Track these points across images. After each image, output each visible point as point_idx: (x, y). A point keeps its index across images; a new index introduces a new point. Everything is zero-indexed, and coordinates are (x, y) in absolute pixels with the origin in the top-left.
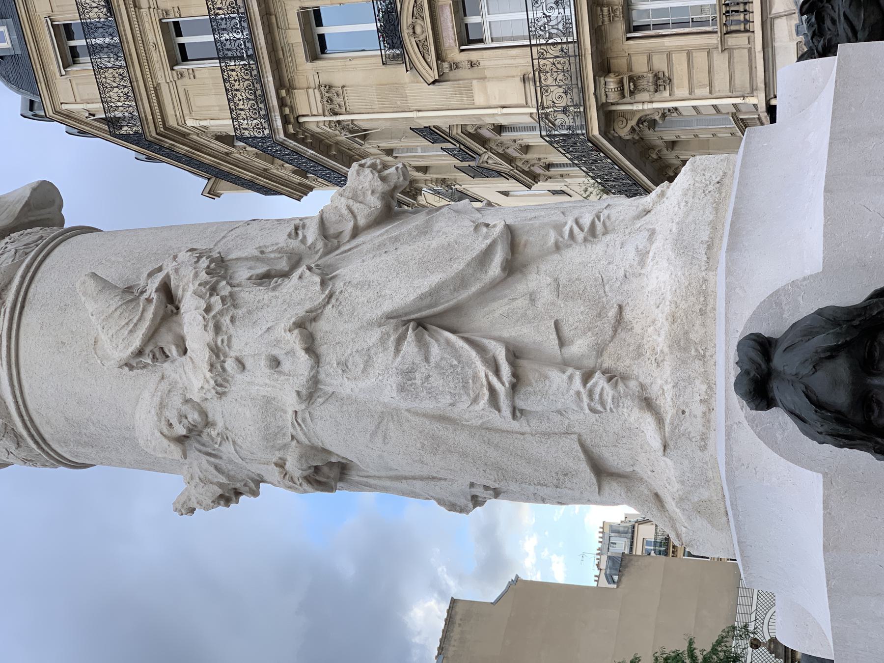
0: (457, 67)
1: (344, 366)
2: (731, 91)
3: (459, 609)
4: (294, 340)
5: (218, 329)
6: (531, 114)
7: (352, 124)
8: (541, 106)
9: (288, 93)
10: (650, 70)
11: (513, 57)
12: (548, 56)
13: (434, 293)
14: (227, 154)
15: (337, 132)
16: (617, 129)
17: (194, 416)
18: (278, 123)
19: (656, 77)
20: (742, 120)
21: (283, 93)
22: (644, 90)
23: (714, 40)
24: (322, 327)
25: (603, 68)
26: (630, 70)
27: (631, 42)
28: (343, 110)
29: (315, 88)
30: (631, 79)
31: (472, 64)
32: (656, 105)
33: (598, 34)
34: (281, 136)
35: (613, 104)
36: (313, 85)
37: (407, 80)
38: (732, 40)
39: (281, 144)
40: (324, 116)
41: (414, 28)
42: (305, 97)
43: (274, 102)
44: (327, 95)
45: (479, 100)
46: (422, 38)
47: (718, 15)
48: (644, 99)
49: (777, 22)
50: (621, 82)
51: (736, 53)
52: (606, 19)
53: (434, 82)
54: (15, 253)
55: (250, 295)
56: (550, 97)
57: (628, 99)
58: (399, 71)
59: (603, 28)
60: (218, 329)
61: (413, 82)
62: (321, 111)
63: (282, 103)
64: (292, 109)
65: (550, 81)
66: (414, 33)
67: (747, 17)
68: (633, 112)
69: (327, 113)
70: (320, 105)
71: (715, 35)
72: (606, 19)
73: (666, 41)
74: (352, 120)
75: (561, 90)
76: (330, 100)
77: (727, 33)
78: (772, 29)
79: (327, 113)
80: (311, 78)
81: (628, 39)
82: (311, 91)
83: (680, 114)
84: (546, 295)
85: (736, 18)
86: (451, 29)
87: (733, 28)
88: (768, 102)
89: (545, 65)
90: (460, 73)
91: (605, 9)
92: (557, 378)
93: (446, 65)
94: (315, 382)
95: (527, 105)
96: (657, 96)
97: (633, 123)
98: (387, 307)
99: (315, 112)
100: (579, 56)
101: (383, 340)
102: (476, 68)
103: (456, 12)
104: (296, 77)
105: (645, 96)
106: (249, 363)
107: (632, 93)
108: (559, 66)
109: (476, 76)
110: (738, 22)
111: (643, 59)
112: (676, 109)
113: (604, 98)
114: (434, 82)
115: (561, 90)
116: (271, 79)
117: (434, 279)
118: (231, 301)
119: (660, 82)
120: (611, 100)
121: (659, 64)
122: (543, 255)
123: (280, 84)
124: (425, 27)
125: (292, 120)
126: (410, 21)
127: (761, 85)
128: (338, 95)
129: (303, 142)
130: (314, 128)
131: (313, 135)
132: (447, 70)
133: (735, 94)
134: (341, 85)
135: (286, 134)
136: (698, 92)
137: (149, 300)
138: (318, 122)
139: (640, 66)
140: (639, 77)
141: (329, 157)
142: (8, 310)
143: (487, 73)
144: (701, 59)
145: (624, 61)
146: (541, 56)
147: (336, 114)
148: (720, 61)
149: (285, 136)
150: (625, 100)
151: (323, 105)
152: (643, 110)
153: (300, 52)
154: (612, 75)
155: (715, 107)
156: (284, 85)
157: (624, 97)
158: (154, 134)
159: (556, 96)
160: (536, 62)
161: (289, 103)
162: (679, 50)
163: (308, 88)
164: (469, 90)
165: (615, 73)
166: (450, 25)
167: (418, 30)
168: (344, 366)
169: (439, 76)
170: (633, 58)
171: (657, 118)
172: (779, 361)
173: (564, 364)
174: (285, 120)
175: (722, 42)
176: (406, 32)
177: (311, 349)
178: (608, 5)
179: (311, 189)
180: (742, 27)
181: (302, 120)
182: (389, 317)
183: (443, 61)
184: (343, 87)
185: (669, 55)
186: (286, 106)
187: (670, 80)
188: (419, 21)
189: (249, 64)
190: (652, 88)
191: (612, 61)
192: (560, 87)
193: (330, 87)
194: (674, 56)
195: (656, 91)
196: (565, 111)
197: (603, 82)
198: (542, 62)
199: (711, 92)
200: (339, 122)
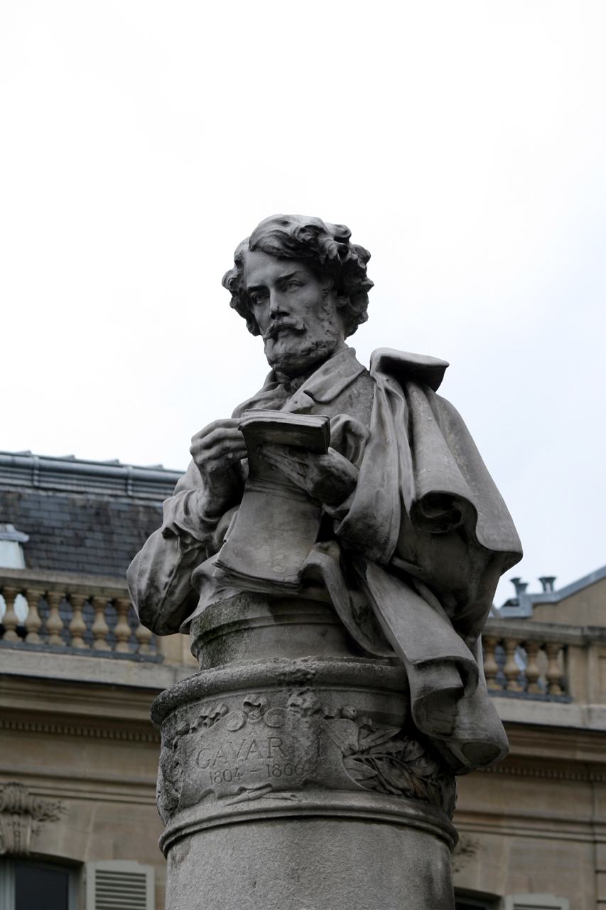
54: (371, 778)
142: (289, 803)
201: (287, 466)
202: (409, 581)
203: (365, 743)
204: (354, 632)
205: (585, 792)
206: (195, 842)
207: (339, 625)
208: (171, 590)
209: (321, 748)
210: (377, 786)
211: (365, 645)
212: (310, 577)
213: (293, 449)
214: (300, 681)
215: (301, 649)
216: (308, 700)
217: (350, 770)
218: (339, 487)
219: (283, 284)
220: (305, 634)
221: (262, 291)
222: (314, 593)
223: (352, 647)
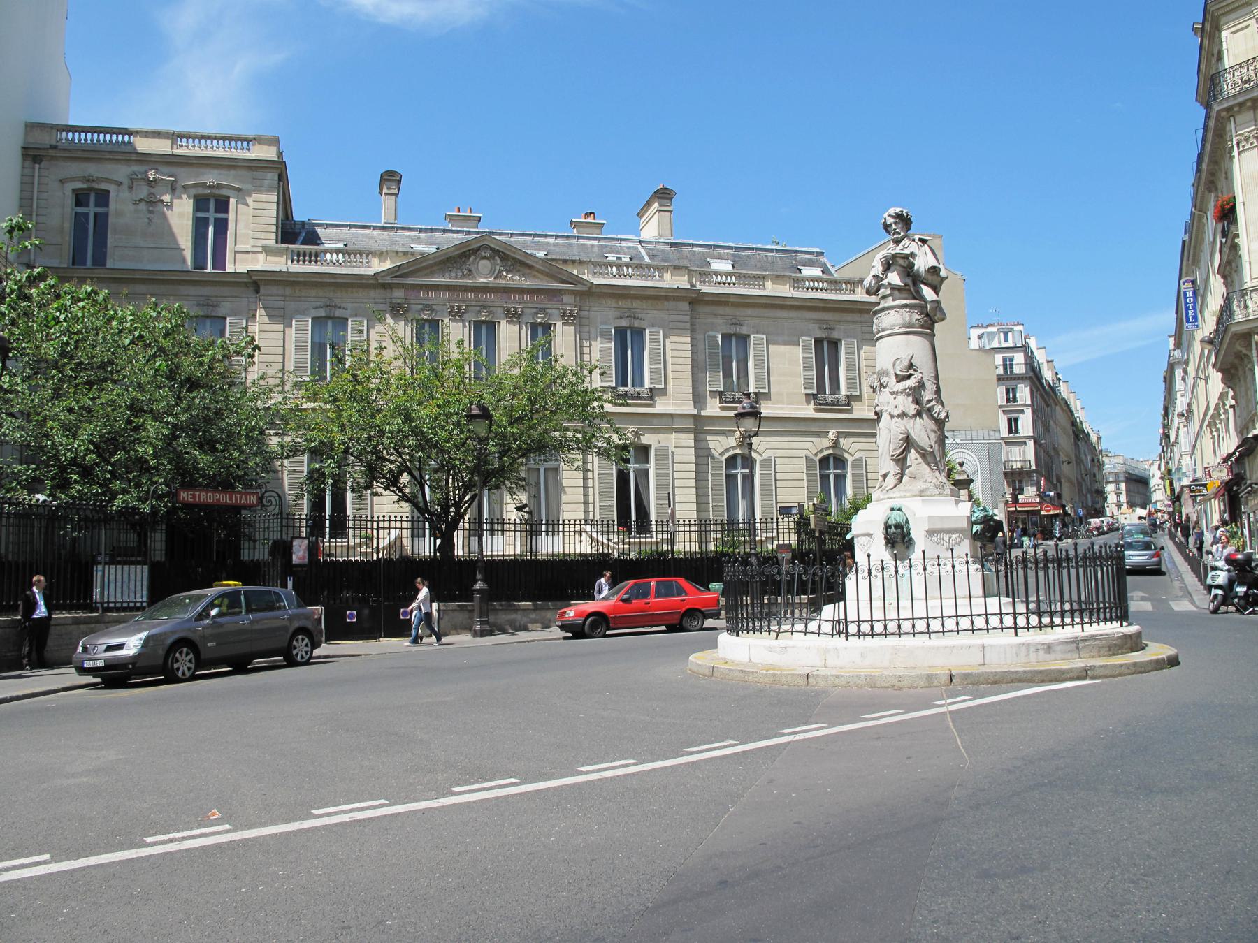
1: (897, 422)
4: (900, 412)
5: (902, 393)
14: (1213, 55)
17: (885, 384)
28: (1241, 149)
55: (910, 398)
60: (902, 393)
64: (1239, 112)
68: (1251, 350)
84: (917, 462)
97: (1244, 351)
135: (1218, 112)
147: (1238, 144)
151: (1242, 134)
158: (1212, 9)
181: (1232, 119)
186: (1240, 107)
201: (901, 262)
202: (925, 284)
203: (919, 317)
207: (912, 293)
210: (922, 327)
213: (903, 258)
219: (895, 223)
221: (891, 225)
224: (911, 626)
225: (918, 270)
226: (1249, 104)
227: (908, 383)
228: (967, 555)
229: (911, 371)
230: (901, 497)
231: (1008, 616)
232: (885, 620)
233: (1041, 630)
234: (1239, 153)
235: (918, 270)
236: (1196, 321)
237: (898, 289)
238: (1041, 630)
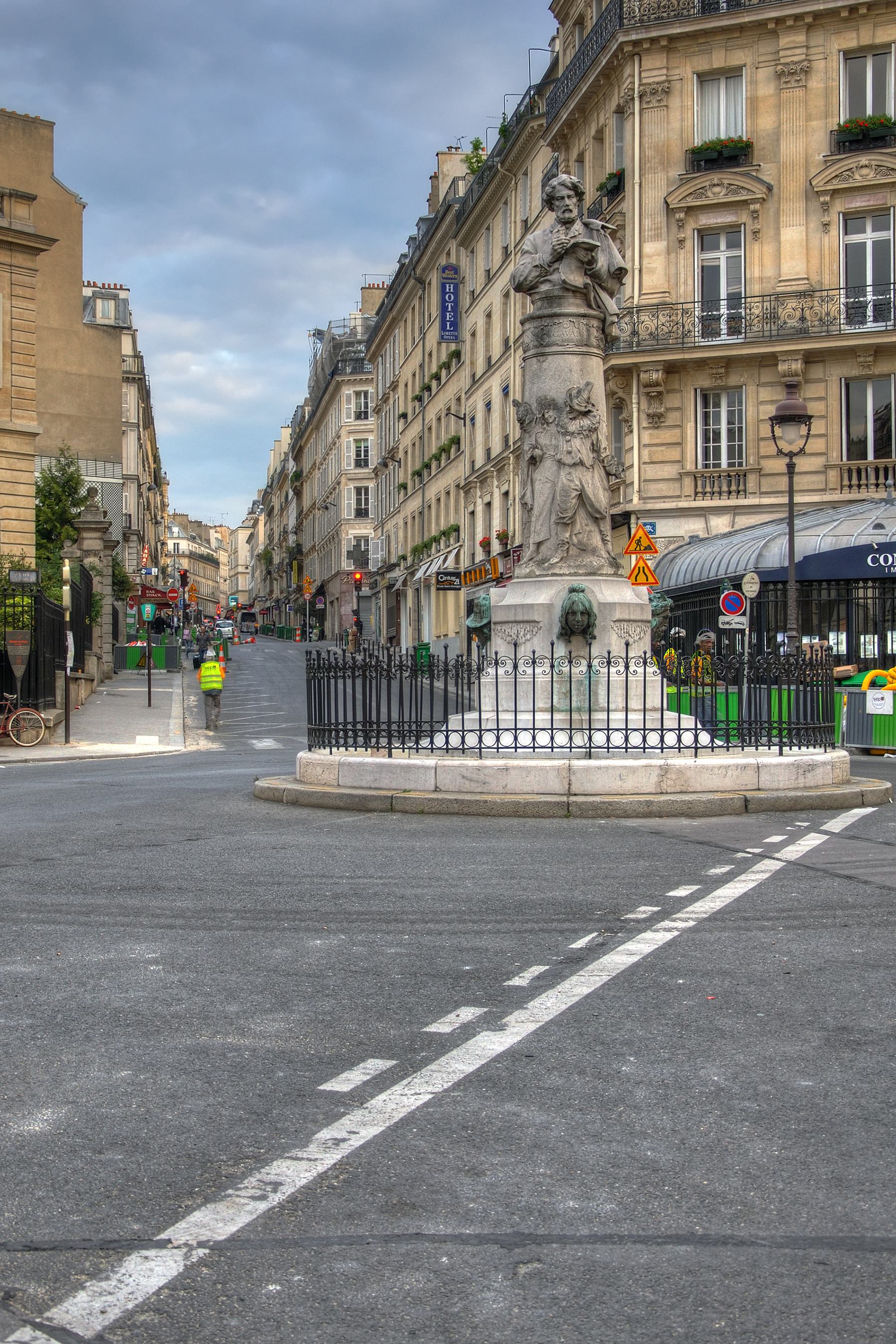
0: (680, 227)
2: (645, 481)
3: (44, 131)
6: (633, 297)
7: (631, 113)
8: (640, 309)
9: (664, 47)
10: (667, 409)
11: (685, 283)
12: (685, 319)
13: (589, 498)
15: (622, 94)
16: (617, 378)
18: (634, 37)
19: (660, 416)
20: (619, 488)
21: (664, 43)
22: (650, 404)
23: (689, 466)
24: (580, 468)
25: (671, 369)
26: (668, 392)
27: (693, 393)
29: (667, 76)
30: (660, 393)
31: (681, 242)
32: (635, 415)
33: (701, 363)
34: (622, 39)
35: (639, 376)
36: (671, 73)
37: (670, 174)
38: (688, 482)
39: (613, 36)
40: (640, 85)
41: (718, 185)
42: (658, 65)
43: (654, 34)
44: (660, 89)
45: (650, 248)
46: (709, 194)
47: (712, 469)
48: (641, 404)
49: (703, 519)
50: (657, 384)
51: (677, 485)
52: (714, 371)
53: (666, 202)
56: (647, 318)
57: (642, 390)
58: (677, 170)
59: (707, 367)
61: (668, 179)
62: (644, 81)
63: (653, 40)
64: (647, 50)
65: (662, 319)
66: (714, 185)
67: (708, 495)
69: (642, 88)
70: (651, 80)
71: (694, 467)
72: (714, 371)
73: (692, 424)
74: (633, 113)
75: (653, 330)
76: (654, 93)
77: (695, 477)
78: (696, 516)
79: (642, 88)
80: (677, 71)
81: (696, 390)
82: (664, 71)
83: (626, 434)
84: (588, 529)
85: (708, 484)
86: (715, 221)
87: (699, 483)
88: (634, 512)
89: (677, 315)
90: (674, 228)
91: (723, 370)
92: (567, 535)
93: (682, 215)
94: (564, 464)
95: (640, 295)
96: (643, 416)
98: (586, 486)
99: (643, 74)
100: (683, 350)
101: (577, 485)
102: (677, 244)
103: (731, 226)
104: (678, 55)
105: (644, 405)
106: (569, 444)
107: (648, 394)
108: (675, 329)
109: (671, 244)
110: (704, 487)
111: (677, 404)
112: (631, 432)
113: (645, 369)
114: (666, 202)
115: (653, 330)
116: (679, 31)
117: (593, 500)
118: (587, 436)
119: (656, 419)
120: (642, 375)
121: (672, 418)
122: (599, 527)
123: (671, 38)
124: (719, 195)
125: (637, 50)
126: (726, 182)
127: (649, 506)
128: (659, 101)
129: (615, 55)
130: (627, 71)
131: (621, 66)
132: (677, 216)
133: (642, 484)
134: (671, 105)
136: (645, 452)
137: (586, 407)
138: (634, 76)
139: (672, 401)
140: (661, 400)
141: (597, 76)
143: (673, 255)
144: (675, 454)
145: (677, 387)
146: (685, 312)
147: (641, 97)
148: (670, 471)
149: (622, 43)
150: (641, 387)
151: (649, 84)
152: (631, 403)
153: (703, 64)
154: (665, 376)
155: (632, 466)
156: (671, 44)
157: (646, 386)
159: (648, 322)
160: (680, 306)
161: (654, 47)
162: (683, 436)
163: (668, 69)
164: (657, 237)
165: (667, 378)
166: (719, 221)
167: (717, 189)
168: (570, 473)
169: (673, 209)
170: (678, 395)
171: (624, 415)
172: (581, 594)
173: (570, 536)
174: (636, 43)
175: (688, 474)
176: (715, 177)
177: (574, 465)
178: (727, 373)
179: (562, 23)
180: (699, 489)
182: (583, 486)
183: (686, 213)
184: (667, 106)
185: (679, 426)
186: (651, 44)
187: (657, 428)
188: (724, 191)
189: (694, 7)
190: (651, 411)
191: (677, 375)
192: (657, 329)
193: (667, 93)
194: (677, 431)
195: (648, 415)
196: (635, 333)
197: (658, 368)
198: (680, 312)
199: (645, 463)
200: (633, 99)
201: (581, 254)
204: (593, 303)
205: (9, 253)
206: (550, 357)
208: (532, 281)
209: (589, 336)
211: (594, 307)
212: (586, 286)
213: (586, 249)
214: (584, 316)
215: (578, 306)
216: (585, 321)
217: (594, 341)
218: (592, 261)
220: (578, 301)
222: (585, 291)
223: (589, 306)
224: (647, 738)
225: (600, 270)
226: (664, 43)
227: (586, 422)
228: (645, 653)
229: (590, 407)
230: (570, 575)
231: (605, 738)
232: (627, 729)
233: (728, 750)
234: (641, 110)
235: (600, 270)
236: (456, 330)
237: (575, 291)
238: (728, 750)
